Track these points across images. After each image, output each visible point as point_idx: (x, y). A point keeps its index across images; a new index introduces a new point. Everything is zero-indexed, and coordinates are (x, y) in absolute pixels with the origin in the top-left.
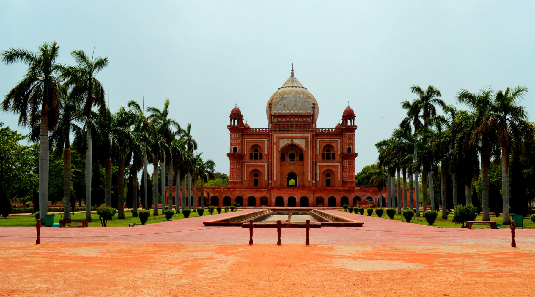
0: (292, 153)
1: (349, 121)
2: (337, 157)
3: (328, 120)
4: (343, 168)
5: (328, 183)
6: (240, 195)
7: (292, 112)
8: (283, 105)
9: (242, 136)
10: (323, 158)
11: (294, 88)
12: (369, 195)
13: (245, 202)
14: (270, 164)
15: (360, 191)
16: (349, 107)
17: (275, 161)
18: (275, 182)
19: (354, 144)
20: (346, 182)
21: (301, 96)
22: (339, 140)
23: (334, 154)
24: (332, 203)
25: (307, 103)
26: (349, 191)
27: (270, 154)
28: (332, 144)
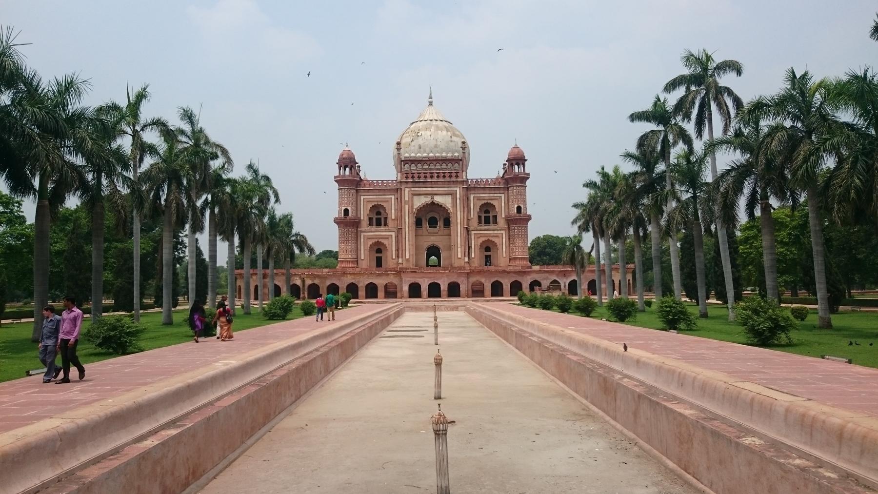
0: (432, 217)
1: (516, 167)
2: (501, 222)
3: (485, 166)
4: (510, 237)
5: (488, 260)
6: (353, 281)
7: (431, 155)
8: (417, 147)
9: (357, 191)
10: (480, 222)
11: (434, 123)
12: (554, 277)
13: (362, 293)
14: (399, 232)
15: (539, 272)
16: (516, 147)
17: (407, 229)
18: (408, 260)
19: (525, 201)
20: (515, 259)
21: (444, 132)
22: (503, 195)
23: (495, 217)
24: (497, 289)
25: (453, 144)
26: (523, 273)
27: (399, 219)
28: (492, 202)
